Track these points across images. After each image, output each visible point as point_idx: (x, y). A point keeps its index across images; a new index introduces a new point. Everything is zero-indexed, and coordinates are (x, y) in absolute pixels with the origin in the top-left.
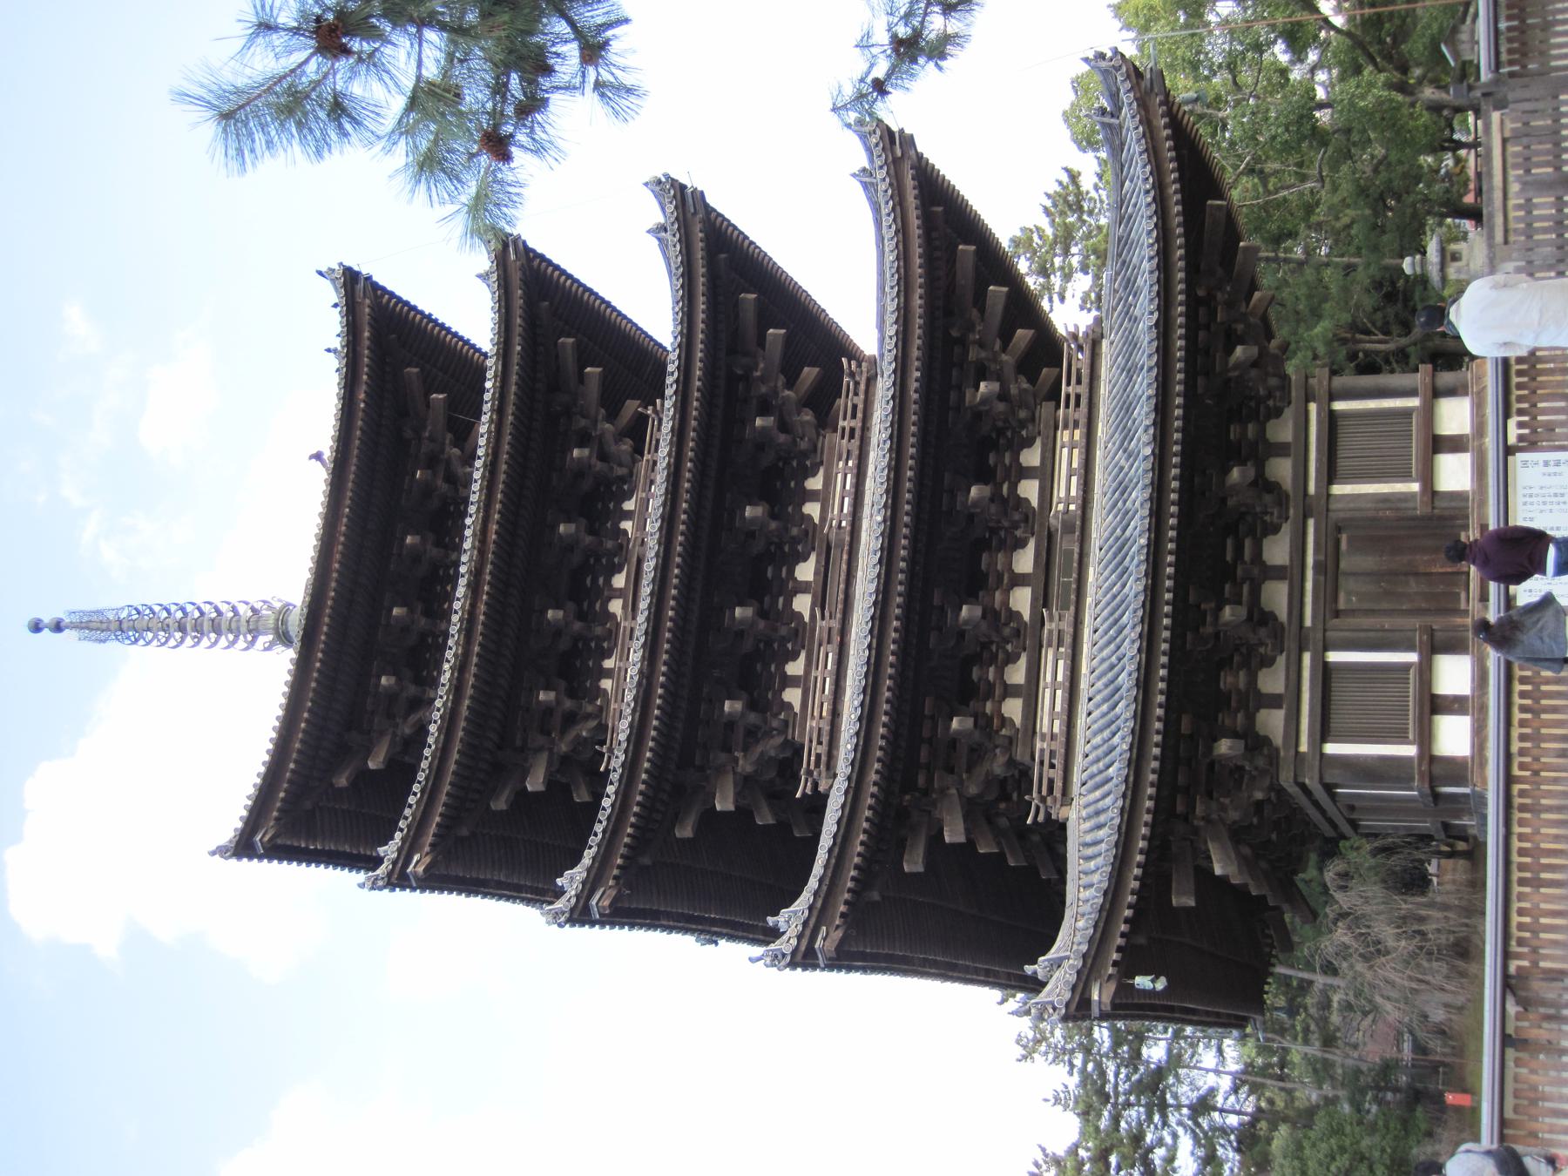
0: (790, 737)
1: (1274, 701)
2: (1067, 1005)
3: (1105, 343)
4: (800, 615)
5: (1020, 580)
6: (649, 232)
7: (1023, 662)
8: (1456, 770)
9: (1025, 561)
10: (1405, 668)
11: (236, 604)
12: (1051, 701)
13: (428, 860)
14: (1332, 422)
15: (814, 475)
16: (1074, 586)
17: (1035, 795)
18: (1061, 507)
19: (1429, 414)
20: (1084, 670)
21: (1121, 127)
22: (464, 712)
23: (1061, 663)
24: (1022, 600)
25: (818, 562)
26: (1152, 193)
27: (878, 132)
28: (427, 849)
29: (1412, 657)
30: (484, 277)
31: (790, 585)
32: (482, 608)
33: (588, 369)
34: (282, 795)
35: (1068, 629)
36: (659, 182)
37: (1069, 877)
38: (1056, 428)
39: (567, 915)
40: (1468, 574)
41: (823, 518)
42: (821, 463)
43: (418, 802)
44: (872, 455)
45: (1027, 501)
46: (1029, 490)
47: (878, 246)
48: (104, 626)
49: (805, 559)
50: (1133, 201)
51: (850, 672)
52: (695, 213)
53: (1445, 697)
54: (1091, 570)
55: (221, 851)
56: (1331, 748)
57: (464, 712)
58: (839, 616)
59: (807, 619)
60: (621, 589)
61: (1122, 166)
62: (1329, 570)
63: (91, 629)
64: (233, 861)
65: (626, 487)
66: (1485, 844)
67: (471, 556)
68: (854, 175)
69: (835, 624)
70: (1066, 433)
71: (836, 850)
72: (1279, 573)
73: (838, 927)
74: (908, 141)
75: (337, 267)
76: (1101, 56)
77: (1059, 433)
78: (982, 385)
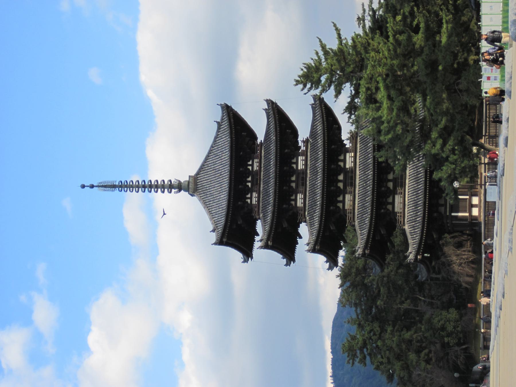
1: (442, 205)
4: (339, 187)
7: (391, 198)
8: (476, 218)
10: (466, 199)
13: (271, 242)
23: (401, 199)
28: (271, 240)
29: (468, 197)
30: (266, 110)
35: (403, 191)
36: (314, 95)
37: (408, 239)
42: (342, 153)
49: (340, 175)
53: (474, 204)
55: (215, 244)
56: (453, 214)
59: (342, 187)
64: (218, 246)
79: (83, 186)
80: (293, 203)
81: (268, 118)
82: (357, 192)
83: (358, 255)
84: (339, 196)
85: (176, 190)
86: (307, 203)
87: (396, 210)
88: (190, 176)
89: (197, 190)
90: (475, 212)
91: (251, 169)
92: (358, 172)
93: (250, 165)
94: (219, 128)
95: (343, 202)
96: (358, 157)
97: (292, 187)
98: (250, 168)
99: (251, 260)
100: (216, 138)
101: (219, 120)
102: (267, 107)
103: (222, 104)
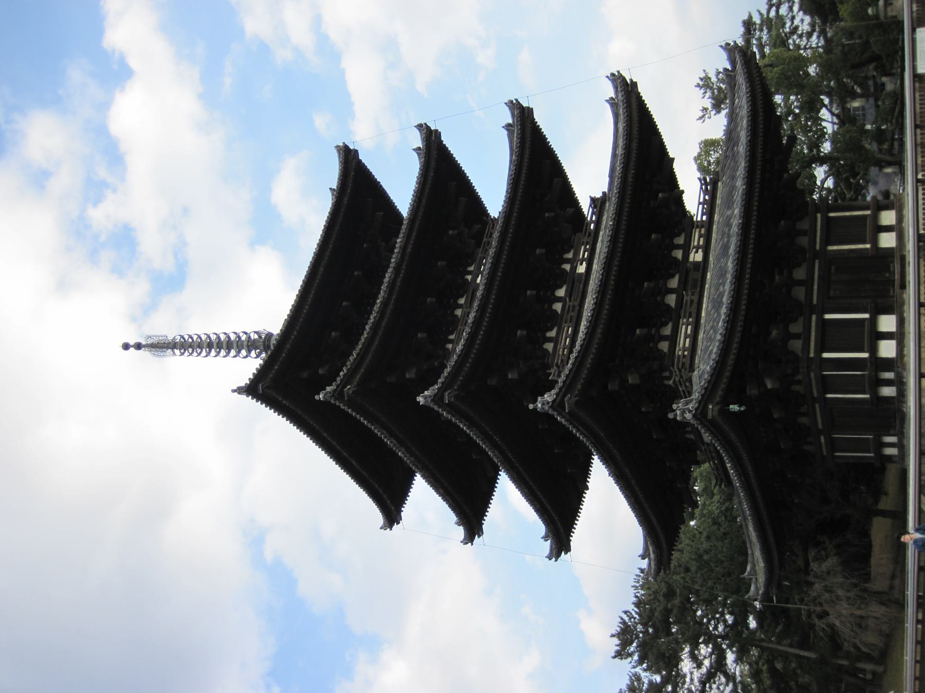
0: (546, 361)
1: (797, 336)
2: (696, 409)
3: (720, 184)
4: (556, 311)
5: (672, 291)
6: (503, 127)
7: (670, 326)
9: (674, 283)
10: (864, 320)
11: (241, 334)
12: (685, 330)
14: (828, 221)
15: (568, 252)
16: (700, 279)
17: (675, 366)
18: (694, 250)
19: (875, 217)
20: (703, 314)
21: (735, 77)
22: (384, 324)
24: (671, 299)
26: (750, 93)
27: (621, 78)
28: (355, 383)
29: (867, 316)
31: (552, 297)
32: (399, 280)
33: (461, 199)
34: (276, 367)
35: (695, 298)
38: (693, 228)
39: (432, 398)
40: (894, 281)
41: (571, 268)
43: (355, 360)
44: (599, 245)
45: (676, 258)
46: (679, 254)
47: (614, 135)
48: (166, 345)
49: (561, 287)
50: (740, 104)
52: (528, 117)
55: (240, 390)
56: (826, 355)
57: (384, 324)
59: (559, 311)
60: (462, 305)
61: (734, 96)
62: (825, 279)
63: (158, 347)
65: (470, 261)
66: (903, 22)
67: (397, 256)
68: (606, 101)
69: (576, 303)
70: (698, 230)
71: (579, 359)
72: (800, 283)
73: (576, 396)
74: (634, 85)
75: (341, 144)
76: (728, 44)
77: (694, 230)
78: (660, 195)
79: (126, 347)
83: (543, 404)
84: (551, 329)
90: (887, 349)
95: (555, 340)
96: (600, 239)
97: (457, 316)
99: (397, 524)
101: (335, 187)
103: (340, 146)
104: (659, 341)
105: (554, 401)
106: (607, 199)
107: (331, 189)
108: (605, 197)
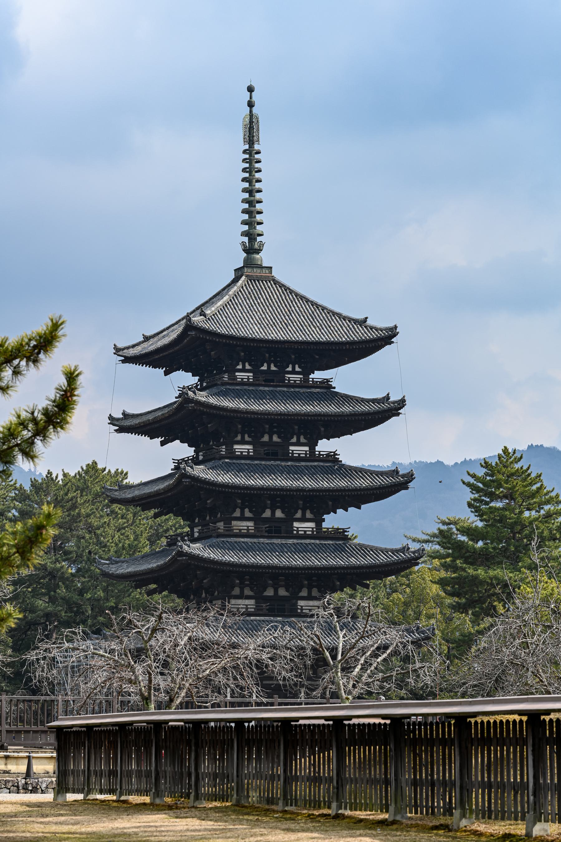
7: (251, 593)
9: (282, 592)
15: (311, 513)
20: (252, 618)
23: (253, 610)
24: (270, 592)
25: (282, 518)
30: (387, 397)
36: (412, 475)
42: (314, 516)
46: (304, 593)
49: (283, 512)
51: (249, 539)
54: (281, 618)
58: (267, 534)
59: (264, 515)
80: (239, 438)
81: (374, 401)
82: (262, 540)
83: (180, 546)
85: (247, 245)
86: (243, 462)
87: (233, 601)
88: (271, 268)
89: (250, 281)
91: (288, 369)
92: (290, 541)
93: (294, 368)
94: (356, 321)
96: (313, 541)
97: (263, 437)
98: (290, 369)
100: (339, 315)
101: (369, 322)
102: (392, 399)
103: (396, 329)
104: (240, 588)
105: (182, 551)
106: (345, 542)
107: (366, 318)
108: (346, 539)
